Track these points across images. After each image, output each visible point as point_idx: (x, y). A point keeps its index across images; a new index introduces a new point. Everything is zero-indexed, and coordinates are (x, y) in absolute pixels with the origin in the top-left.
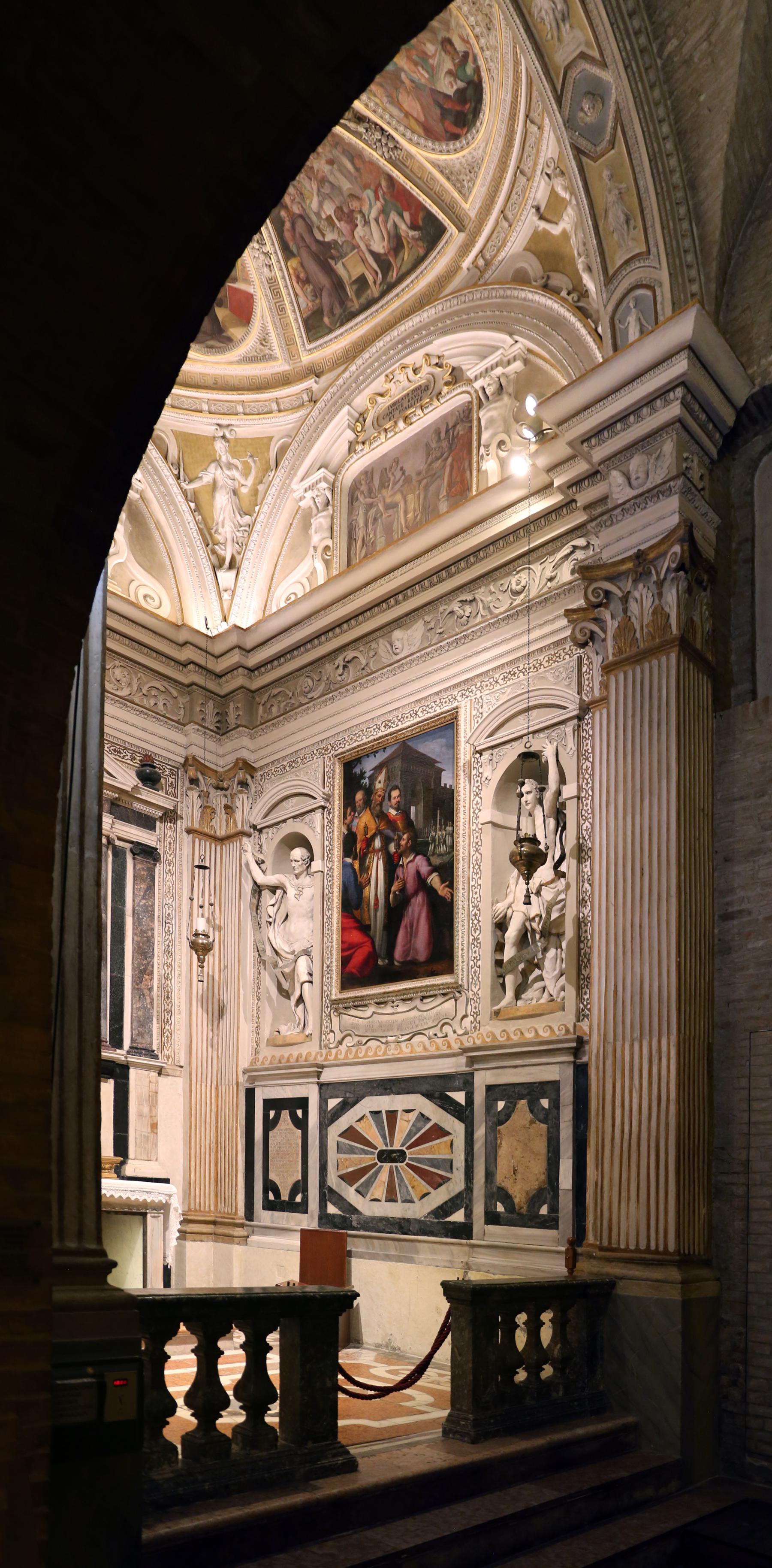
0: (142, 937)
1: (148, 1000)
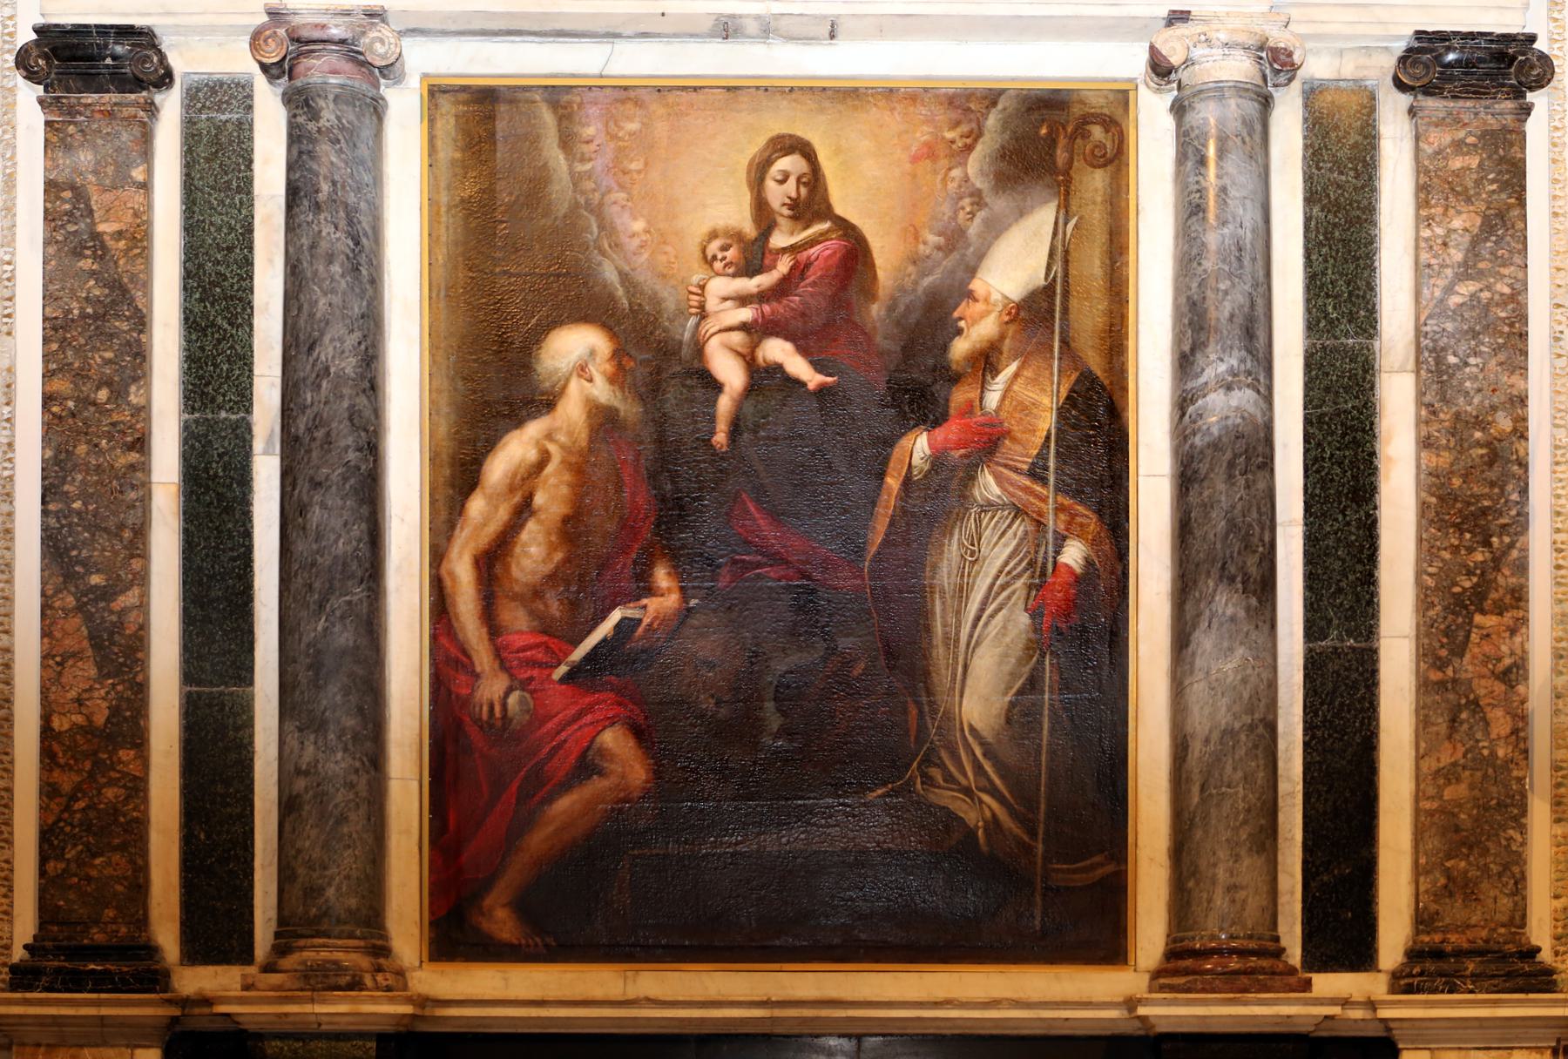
0: (1462, 447)
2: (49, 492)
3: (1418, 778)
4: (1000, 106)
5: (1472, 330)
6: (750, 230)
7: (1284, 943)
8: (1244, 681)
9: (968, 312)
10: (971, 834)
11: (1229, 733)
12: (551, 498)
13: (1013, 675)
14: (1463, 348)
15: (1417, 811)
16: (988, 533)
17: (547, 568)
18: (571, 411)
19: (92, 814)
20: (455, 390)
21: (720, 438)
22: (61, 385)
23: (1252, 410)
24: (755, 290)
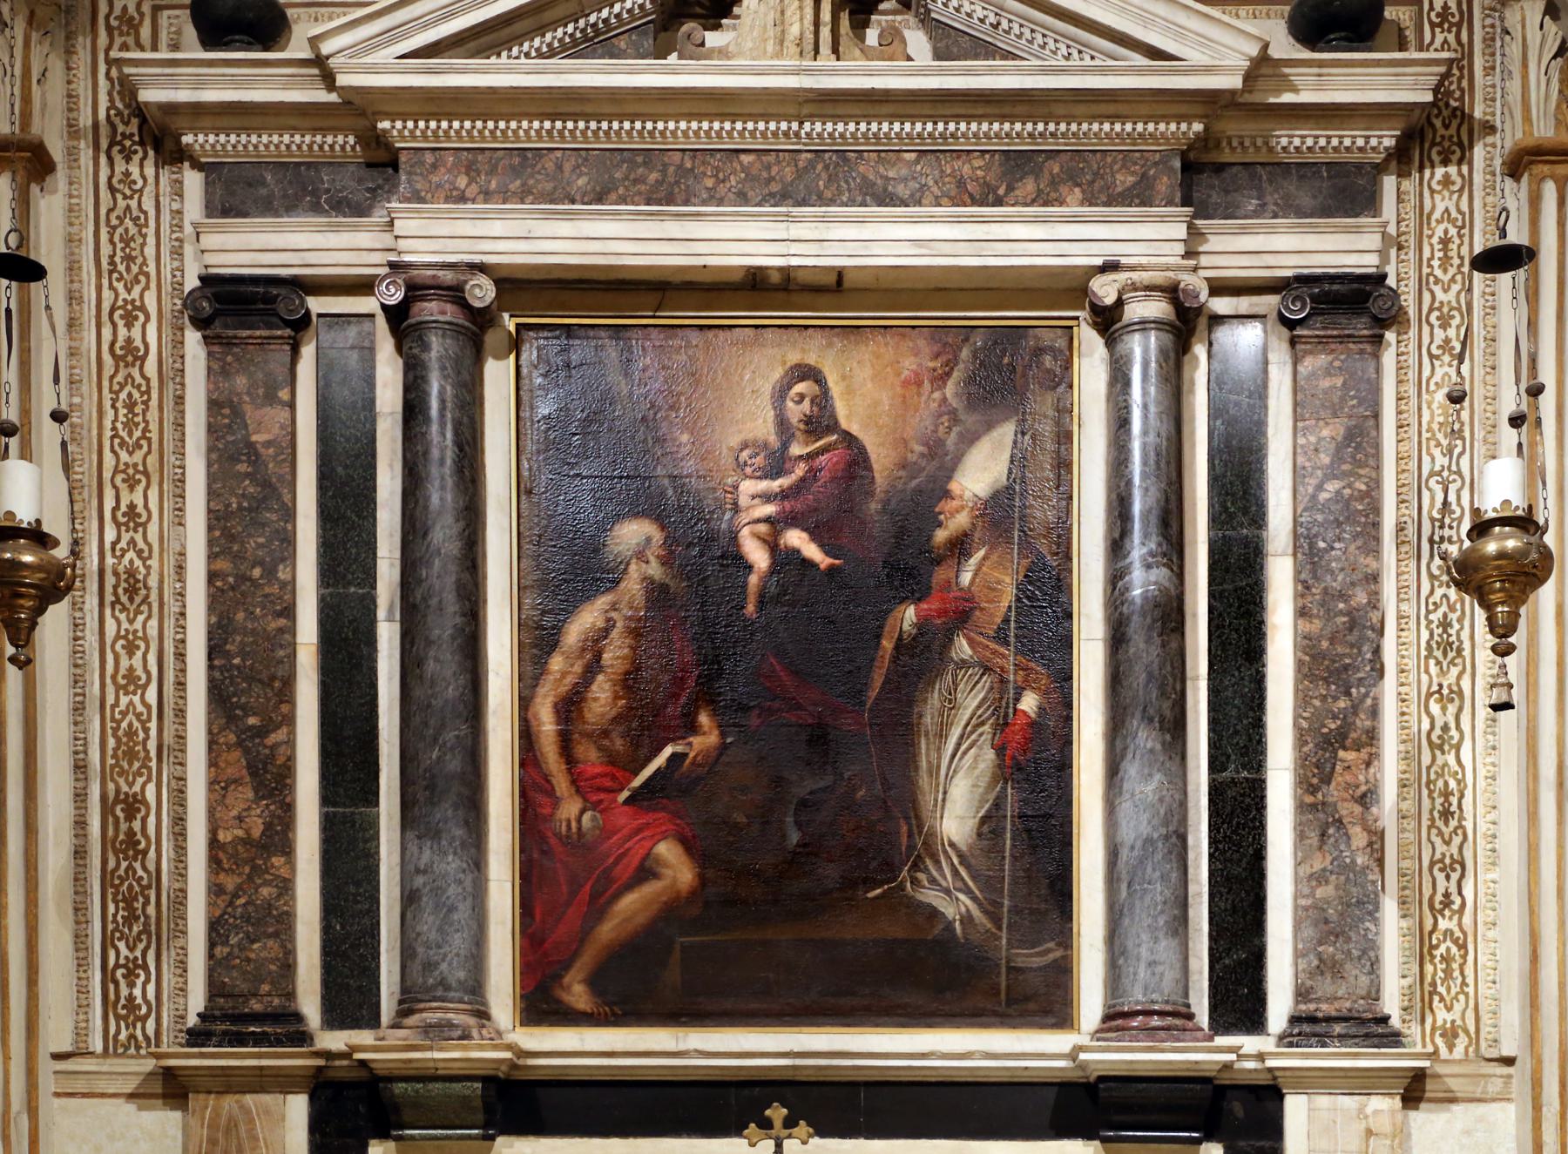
0: (1330, 614)
1: (1359, 838)
2: (213, 651)
3: (1297, 880)
5: (1337, 520)
6: (773, 440)
7: (1193, 1010)
8: (1161, 800)
10: (949, 926)
11: (1149, 841)
12: (615, 653)
13: (982, 801)
14: (1330, 535)
15: (1296, 907)
17: (613, 713)
18: (632, 585)
19: (250, 908)
21: (750, 608)
22: (223, 565)
23: (1167, 584)
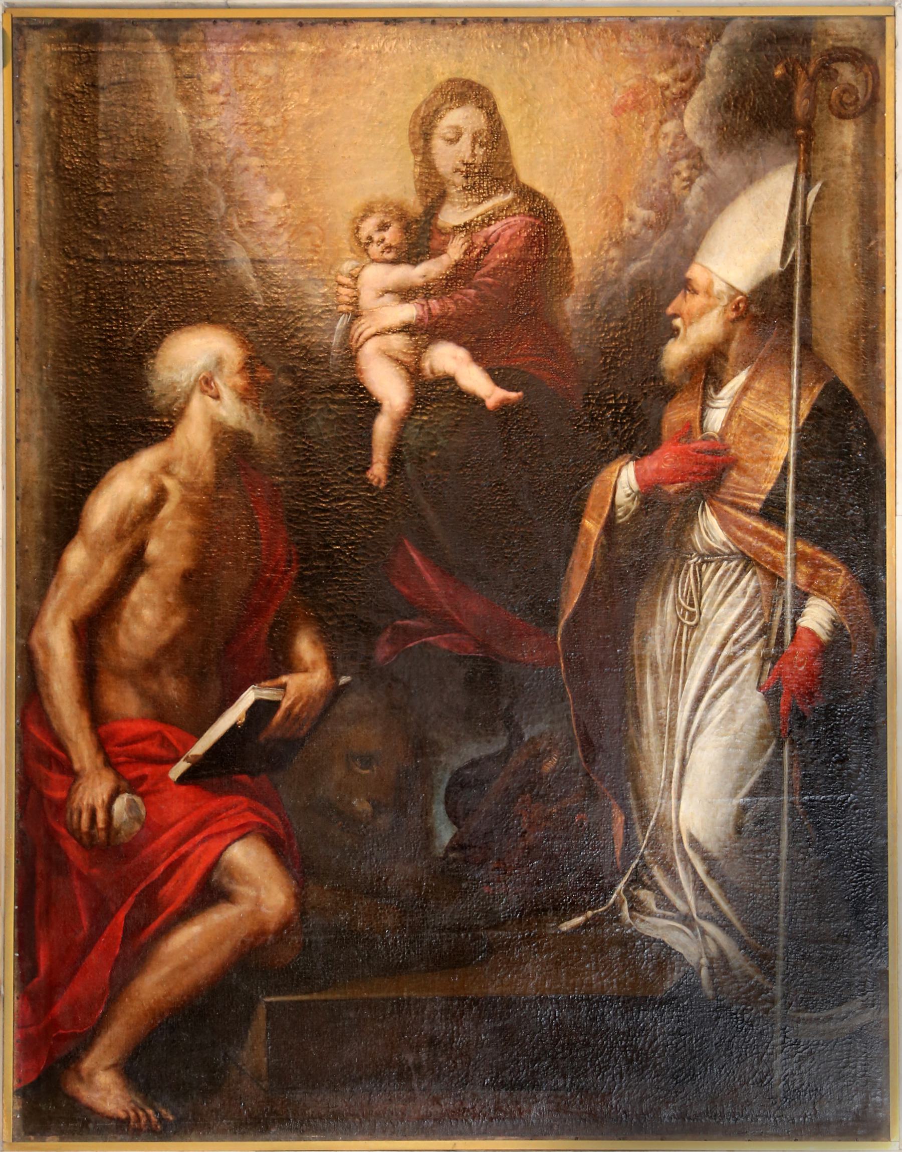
4: (725, 40)
9: (685, 308)
13: (744, 771)
16: (710, 589)
17: (165, 636)
20: (50, 410)
21: (378, 470)
24: (420, 281)
